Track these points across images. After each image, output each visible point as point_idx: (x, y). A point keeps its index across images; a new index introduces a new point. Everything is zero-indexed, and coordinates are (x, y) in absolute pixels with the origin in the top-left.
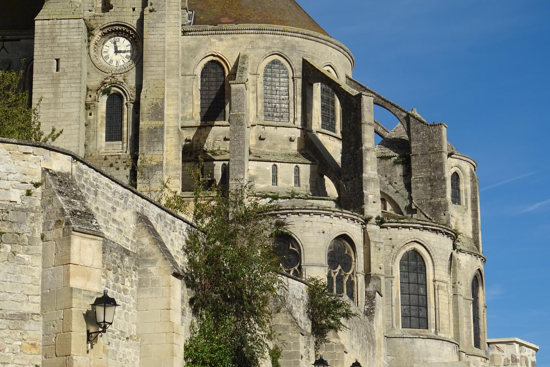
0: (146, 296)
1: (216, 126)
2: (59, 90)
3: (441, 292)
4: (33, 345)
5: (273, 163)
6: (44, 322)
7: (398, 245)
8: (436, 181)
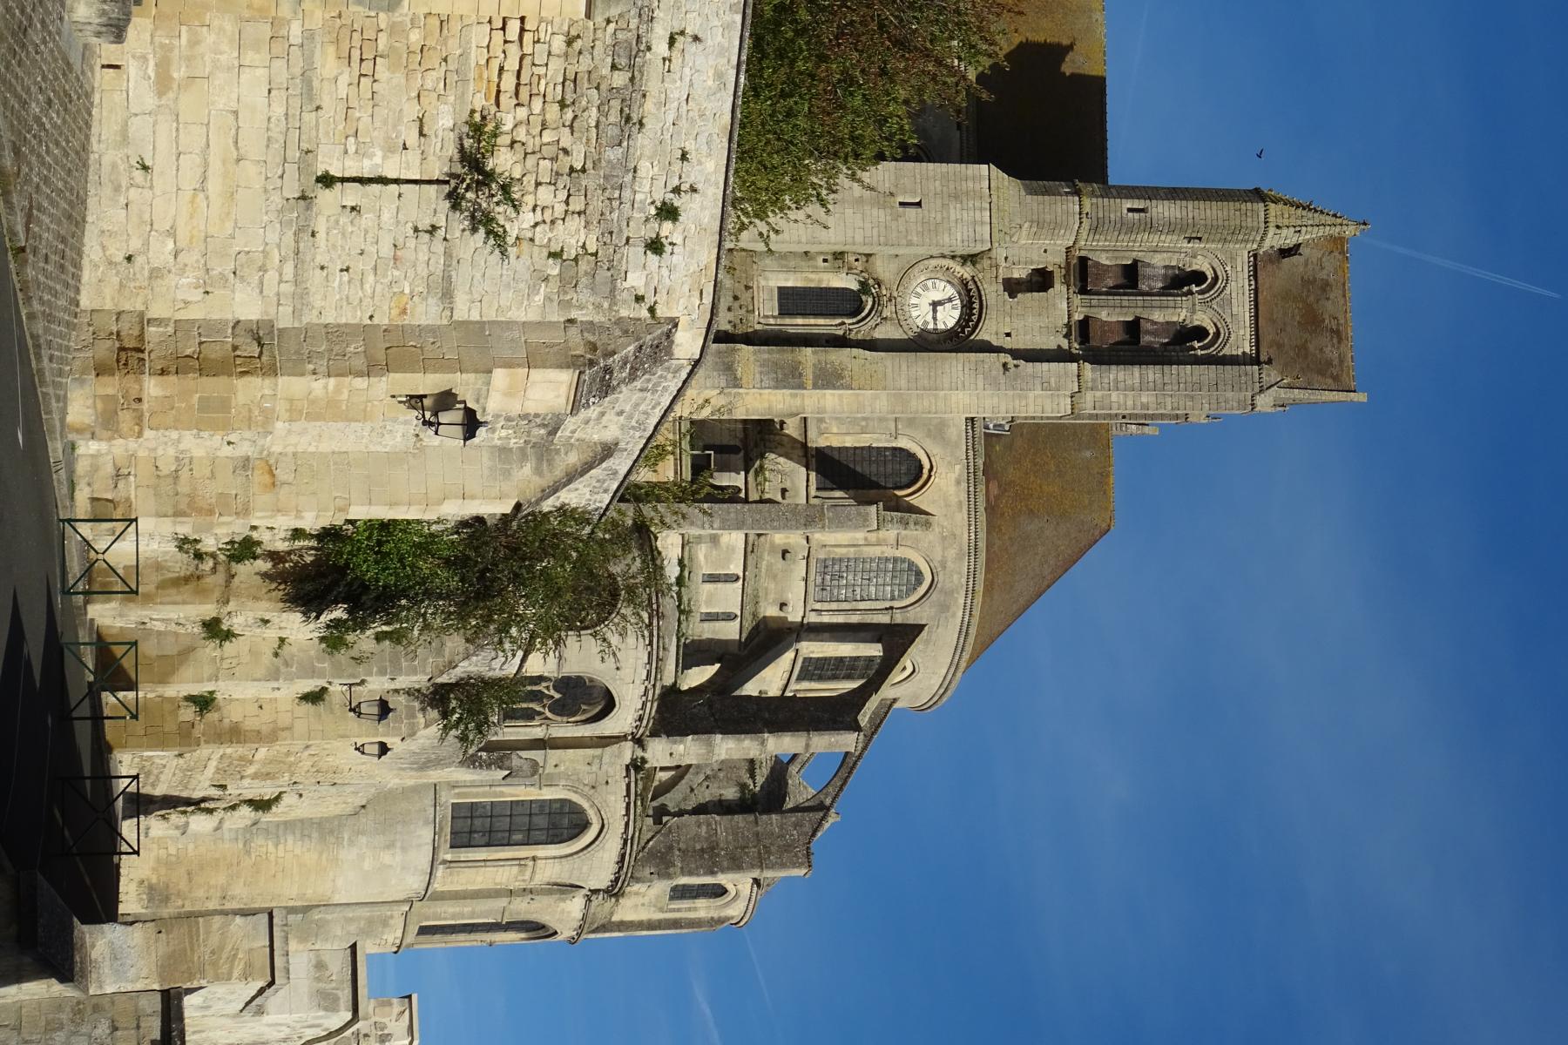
0: (485, 459)
1: (808, 475)
3: (515, 870)
4: (404, 312)
5: (741, 575)
6: (439, 326)
8: (711, 857)
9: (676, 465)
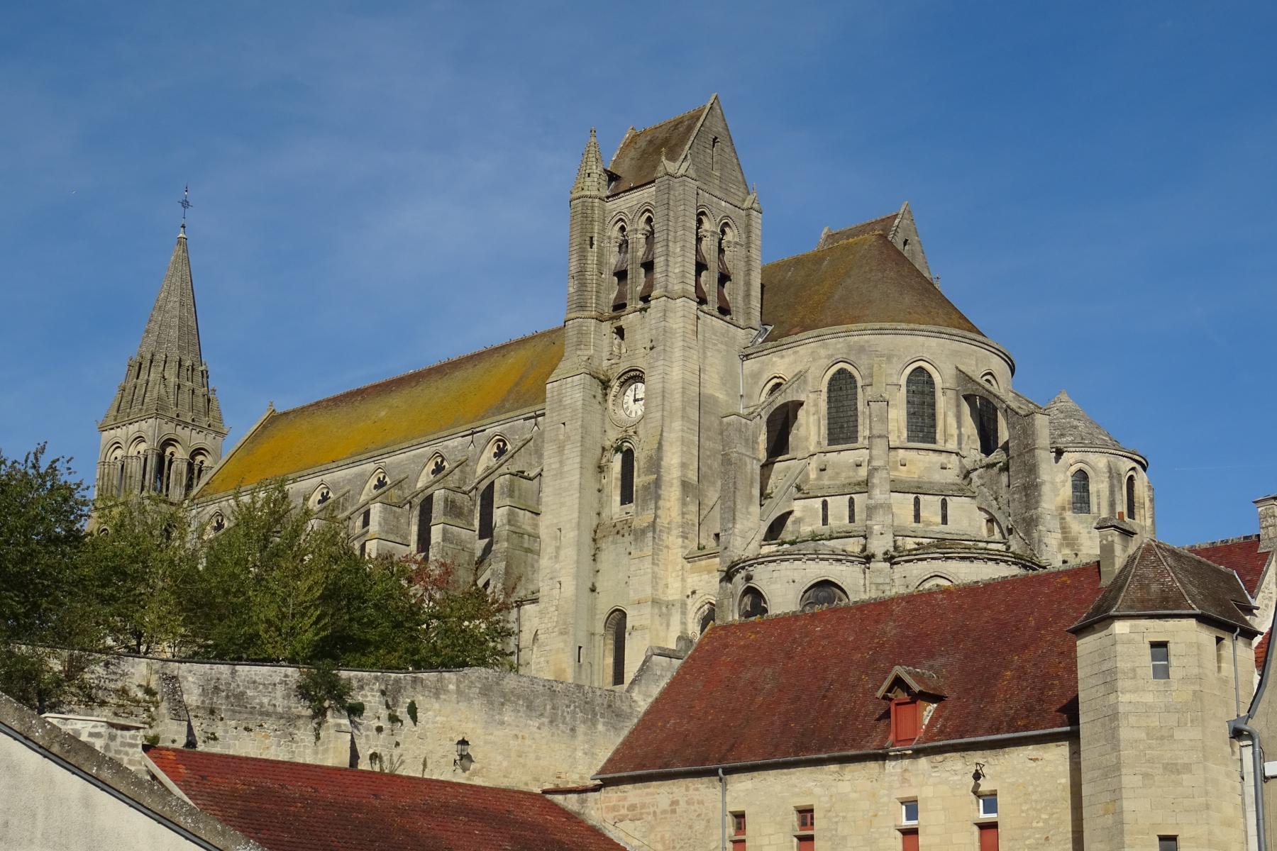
2: (565, 457)
5: (822, 499)
7: (912, 584)
9: (711, 558)
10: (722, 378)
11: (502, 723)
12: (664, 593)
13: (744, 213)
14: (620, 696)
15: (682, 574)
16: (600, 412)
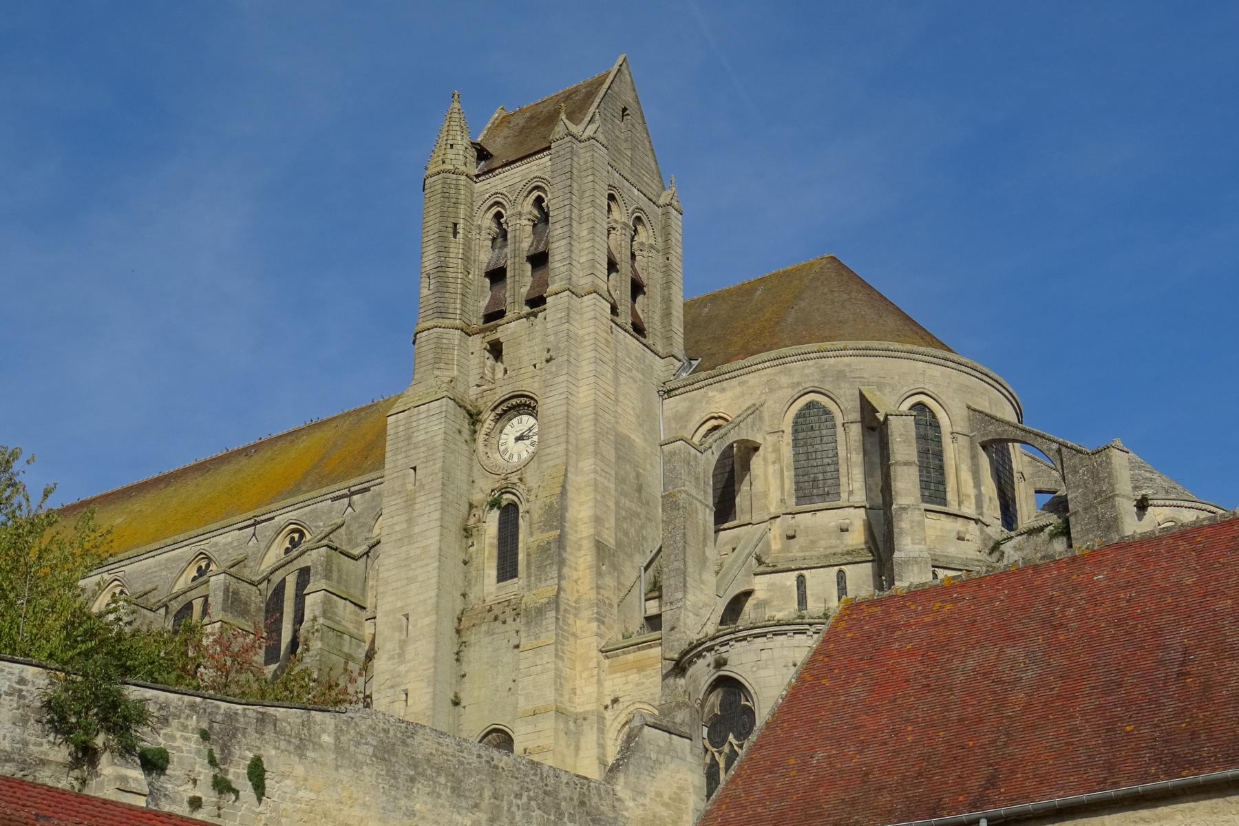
2: (416, 513)
5: (796, 573)
9: (643, 648)
10: (638, 417)
11: (411, 814)
12: (570, 701)
13: (660, 211)
14: (598, 789)
15: (598, 674)
16: (466, 454)
